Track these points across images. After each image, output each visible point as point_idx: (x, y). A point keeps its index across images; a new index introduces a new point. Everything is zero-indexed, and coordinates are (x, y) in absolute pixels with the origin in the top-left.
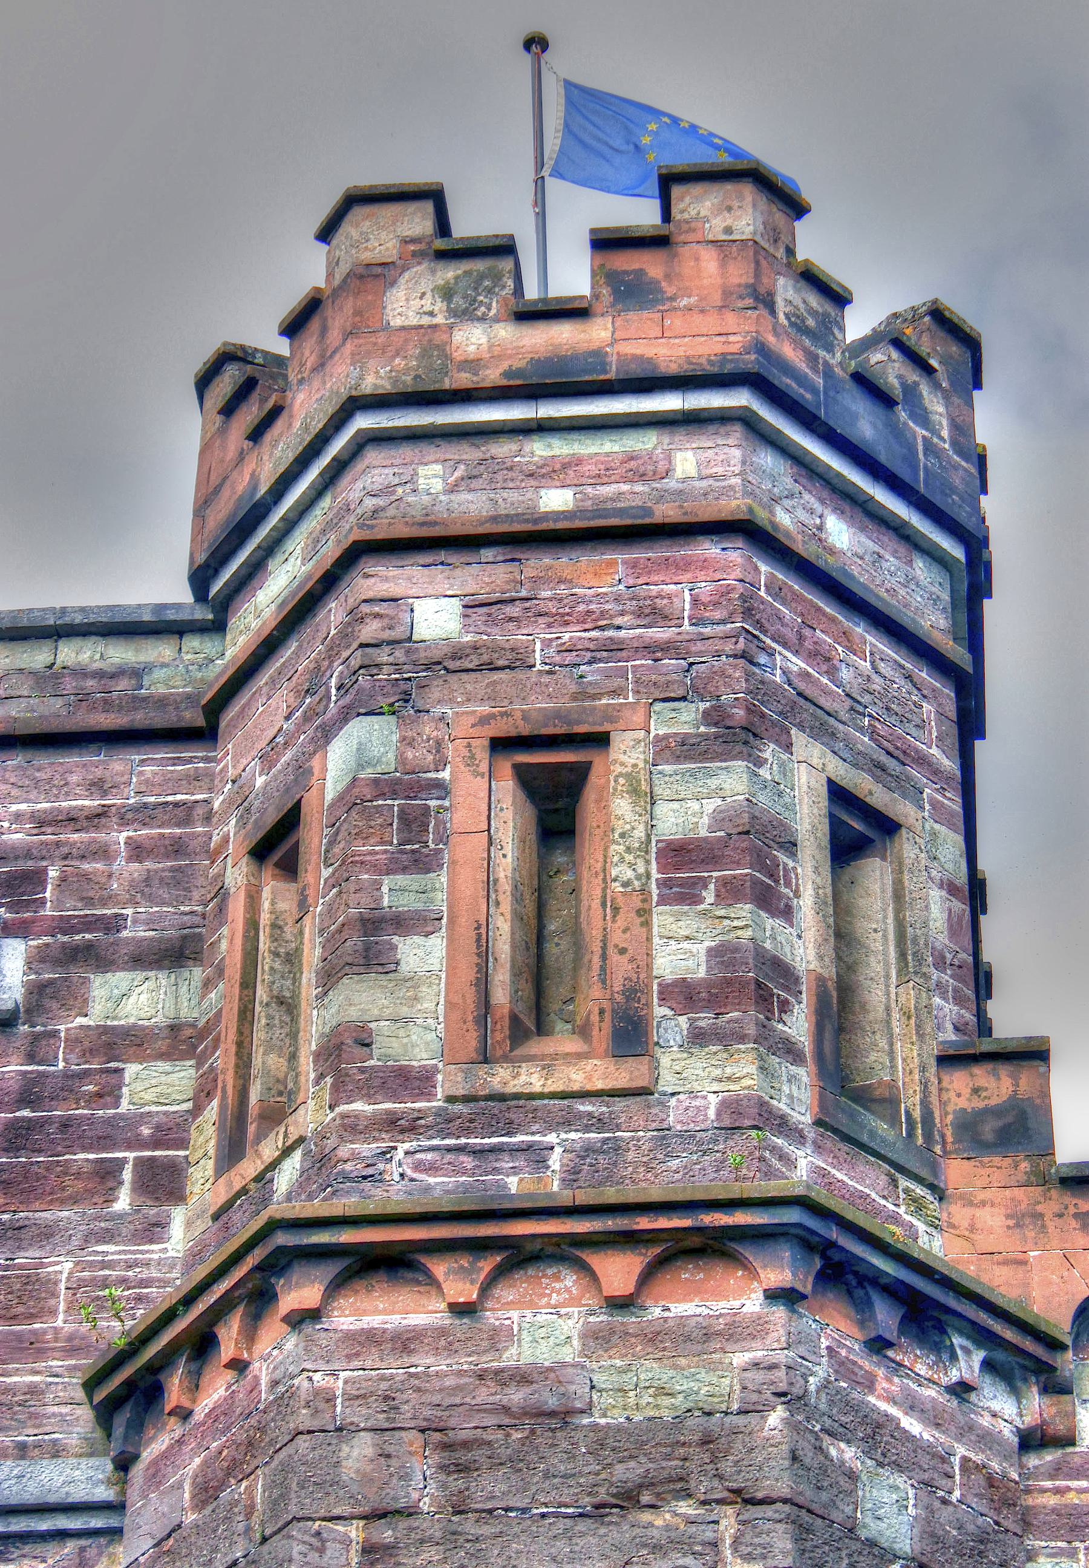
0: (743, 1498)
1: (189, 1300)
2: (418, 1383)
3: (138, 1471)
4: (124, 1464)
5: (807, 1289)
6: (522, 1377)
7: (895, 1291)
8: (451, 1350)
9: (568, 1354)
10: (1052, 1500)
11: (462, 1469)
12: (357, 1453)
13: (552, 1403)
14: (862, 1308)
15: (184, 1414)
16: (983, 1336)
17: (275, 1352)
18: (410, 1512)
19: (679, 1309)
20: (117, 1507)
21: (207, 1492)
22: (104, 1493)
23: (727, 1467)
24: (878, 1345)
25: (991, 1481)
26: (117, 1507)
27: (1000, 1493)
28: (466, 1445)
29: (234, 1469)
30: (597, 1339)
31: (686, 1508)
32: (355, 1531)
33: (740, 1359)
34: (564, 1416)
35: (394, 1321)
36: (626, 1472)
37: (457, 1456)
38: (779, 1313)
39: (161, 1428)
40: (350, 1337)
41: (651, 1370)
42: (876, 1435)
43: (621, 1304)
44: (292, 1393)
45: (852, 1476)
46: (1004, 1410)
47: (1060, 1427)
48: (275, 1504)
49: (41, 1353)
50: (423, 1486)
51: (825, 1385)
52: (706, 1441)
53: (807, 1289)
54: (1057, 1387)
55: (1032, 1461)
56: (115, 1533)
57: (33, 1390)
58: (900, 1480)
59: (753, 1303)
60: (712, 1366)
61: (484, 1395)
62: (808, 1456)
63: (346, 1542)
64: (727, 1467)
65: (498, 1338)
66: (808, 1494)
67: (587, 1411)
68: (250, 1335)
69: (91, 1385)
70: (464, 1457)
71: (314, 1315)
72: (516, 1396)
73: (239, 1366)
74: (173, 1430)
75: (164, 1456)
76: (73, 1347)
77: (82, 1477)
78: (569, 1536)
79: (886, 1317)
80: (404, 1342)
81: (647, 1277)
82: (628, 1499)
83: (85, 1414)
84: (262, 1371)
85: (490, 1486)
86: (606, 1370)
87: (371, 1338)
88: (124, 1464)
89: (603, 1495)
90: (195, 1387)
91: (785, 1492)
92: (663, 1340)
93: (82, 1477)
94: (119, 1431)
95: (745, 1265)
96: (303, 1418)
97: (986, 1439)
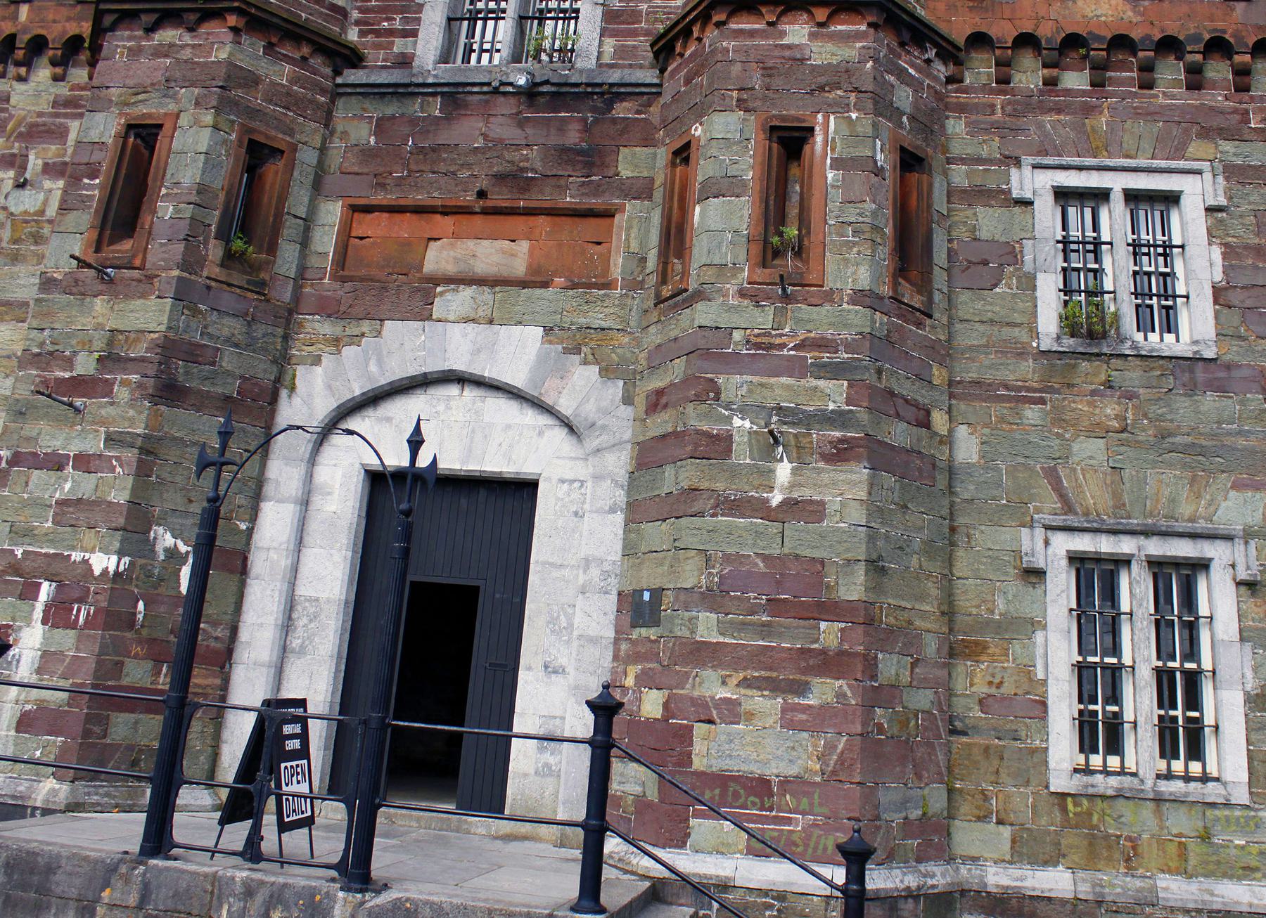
0: (857, 90)
1: (684, 17)
2: (757, 47)
3: (666, 74)
4: (662, 71)
5: (881, 23)
6: (789, 47)
7: (910, 28)
8: (767, 38)
9: (804, 41)
10: (955, 100)
11: (769, 76)
12: (736, 69)
13: (798, 56)
14: (898, 34)
15: (681, 55)
16: (936, 45)
17: (711, 34)
18: (753, 89)
19: (840, 28)
20: (660, 85)
21: (688, 81)
22: (656, 81)
23: (853, 80)
24: (902, 44)
25: (936, 92)
26: (660, 85)
27: (939, 97)
28: (771, 68)
29: (698, 73)
30: (812, 36)
31: (839, 92)
32: (735, 94)
33: (858, 45)
34: (803, 60)
35: (748, 26)
36: (821, 80)
37: (768, 72)
38: (872, 31)
39: (674, 60)
40: (735, 31)
41: (830, 47)
42: (901, 74)
43: (820, 25)
44: (716, 49)
45: (893, 86)
46: (941, 70)
47: (959, 76)
48: (710, 85)
49: (637, 35)
50: (757, 81)
51: (885, 56)
52: (847, 71)
53: (881, 23)
54: (959, 63)
55: (950, 87)
56: (659, 94)
57: (634, 47)
58: (908, 89)
59: (863, 28)
60: (850, 47)
61: (776, 53)
62: (879, 78)
63: (732, 97)
64: (853, 80)
65: (783, 34)
66: (878, 91)
67: (809, 59)
68: (703, 30)
69: (652, 46)
70: (770, 72)
71: (724, 23)
72: (787, 53)
73: (699, 39)
74: (679, 60)
75: (675, 69)
76: (647, 33)
77: (650, 76)
78: (802, 99)
79: (906, 36)
80: (752, 34)
81: (830, 17)
82: (821, 89)
83: (651, 55)
84: (706, 41)
85: (777, 82)
86: (816, 46)
87: (741, 31)
88: (662, 71)
89: (813, 87)
90: (685, 47)
91: (871, 88)
92: (833, 37)
93: (650, 76)
94: (661, 60)
95: (860, 13)
96: (719, 57)
97: (935, 79)
